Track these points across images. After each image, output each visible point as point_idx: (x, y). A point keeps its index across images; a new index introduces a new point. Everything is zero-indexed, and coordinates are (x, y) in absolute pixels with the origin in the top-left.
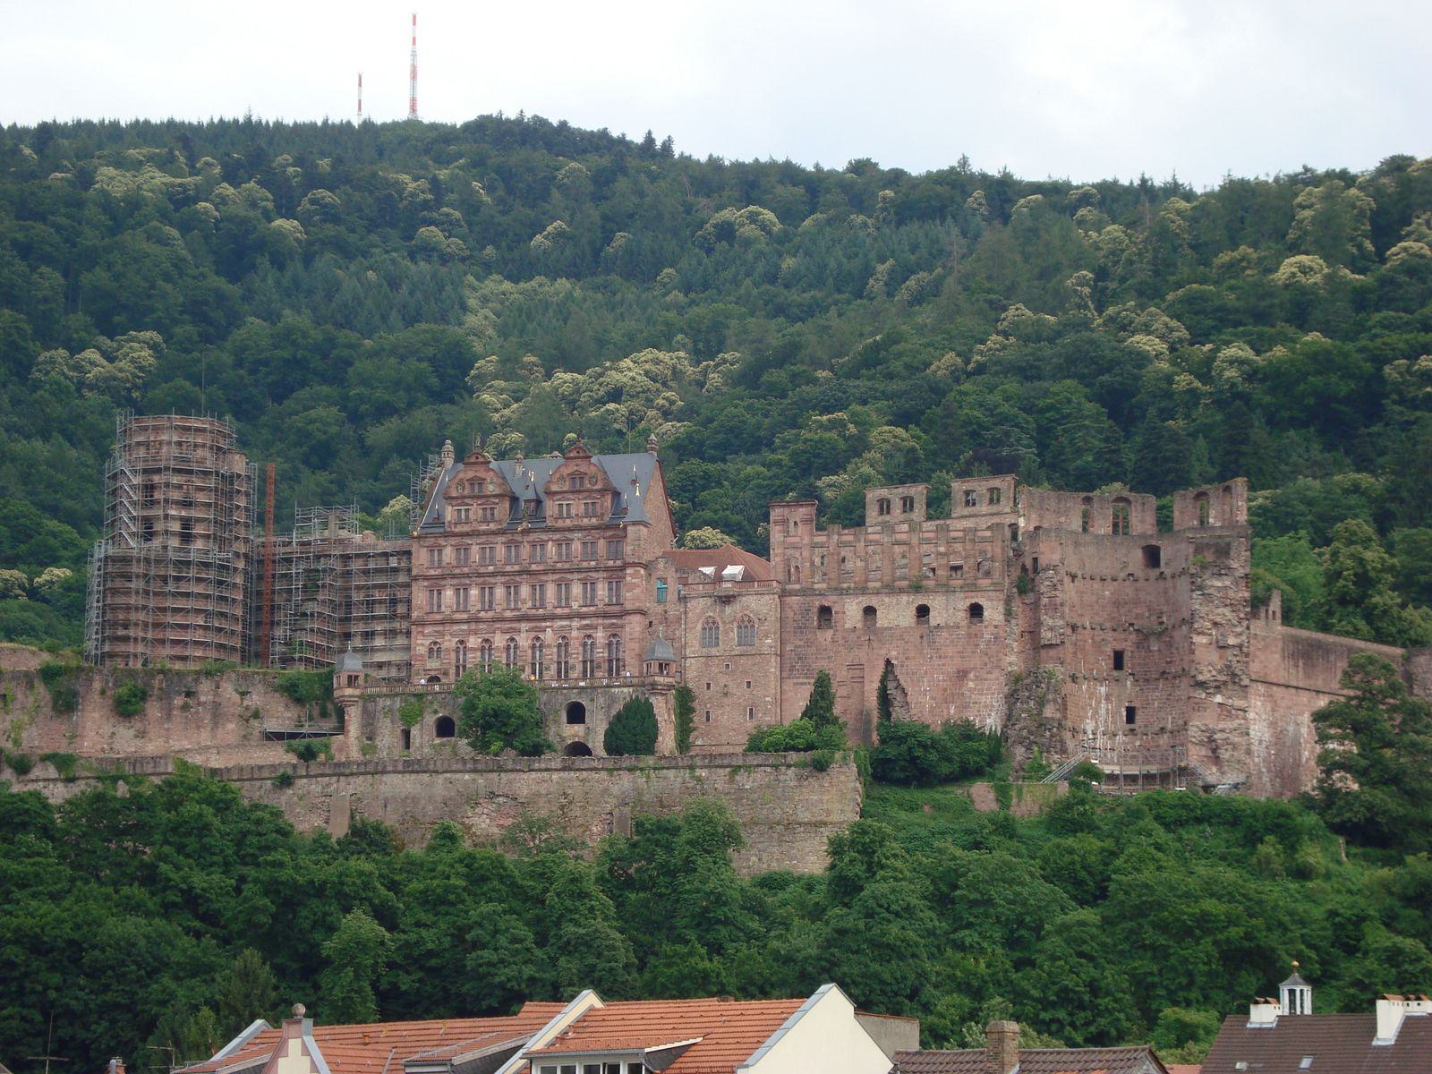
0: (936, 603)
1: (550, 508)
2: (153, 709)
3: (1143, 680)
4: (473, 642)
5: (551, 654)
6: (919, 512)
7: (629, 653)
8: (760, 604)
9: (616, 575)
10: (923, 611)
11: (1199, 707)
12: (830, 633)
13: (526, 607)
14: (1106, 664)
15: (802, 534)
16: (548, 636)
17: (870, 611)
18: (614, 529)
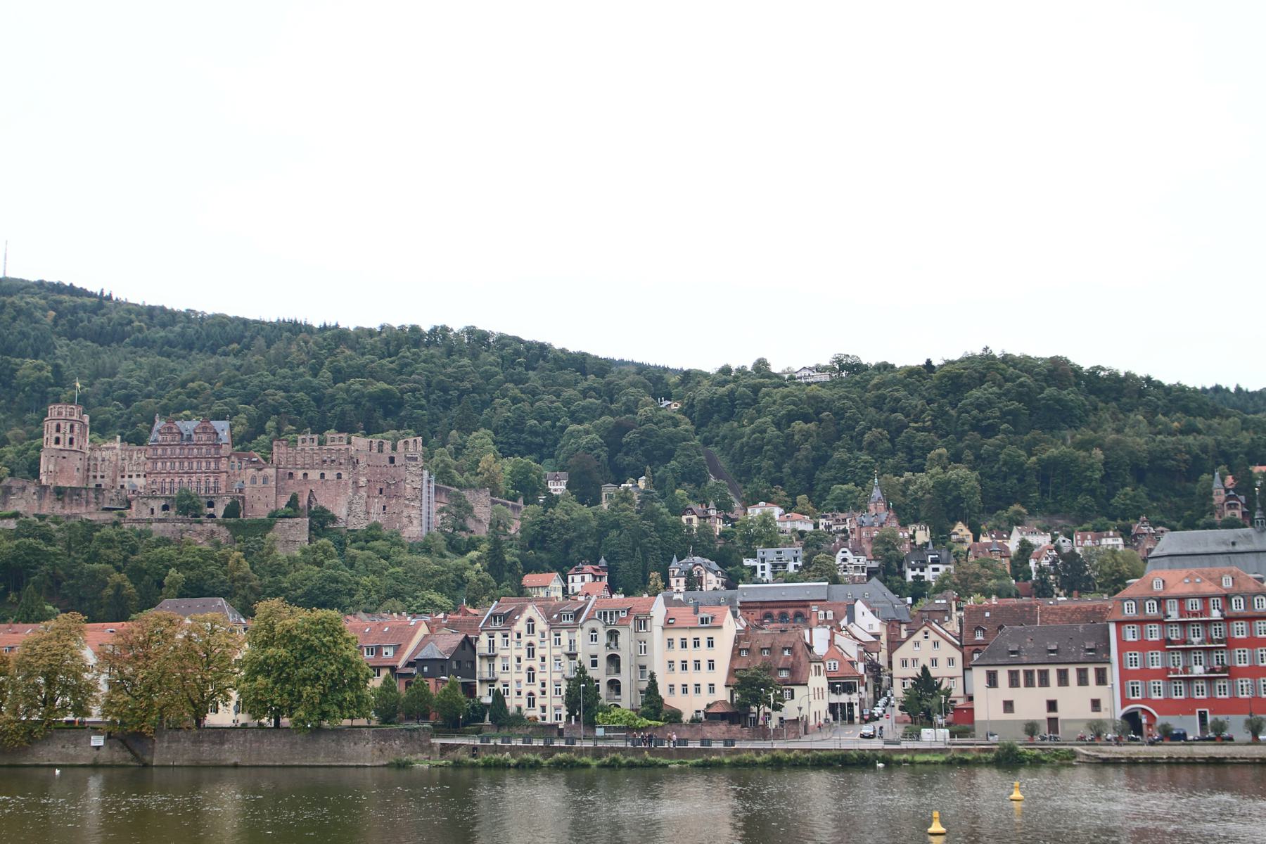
0: (327, 473)
1: (195, 437)
2: (67, 500)
3: (389, 497)
4: (168, 480)
5: (194, 485)
6: (316, 443)
7: (222, 485)
8: (271, 471)
9: (218, 460)
10: (322, 475)
11: (407, 506)
12: (291, 481)
13: (186, 469)
14: (377, 492)
15: (283, 450)
16: (194, 479)
17: (305, 475)
18: (218, 446)
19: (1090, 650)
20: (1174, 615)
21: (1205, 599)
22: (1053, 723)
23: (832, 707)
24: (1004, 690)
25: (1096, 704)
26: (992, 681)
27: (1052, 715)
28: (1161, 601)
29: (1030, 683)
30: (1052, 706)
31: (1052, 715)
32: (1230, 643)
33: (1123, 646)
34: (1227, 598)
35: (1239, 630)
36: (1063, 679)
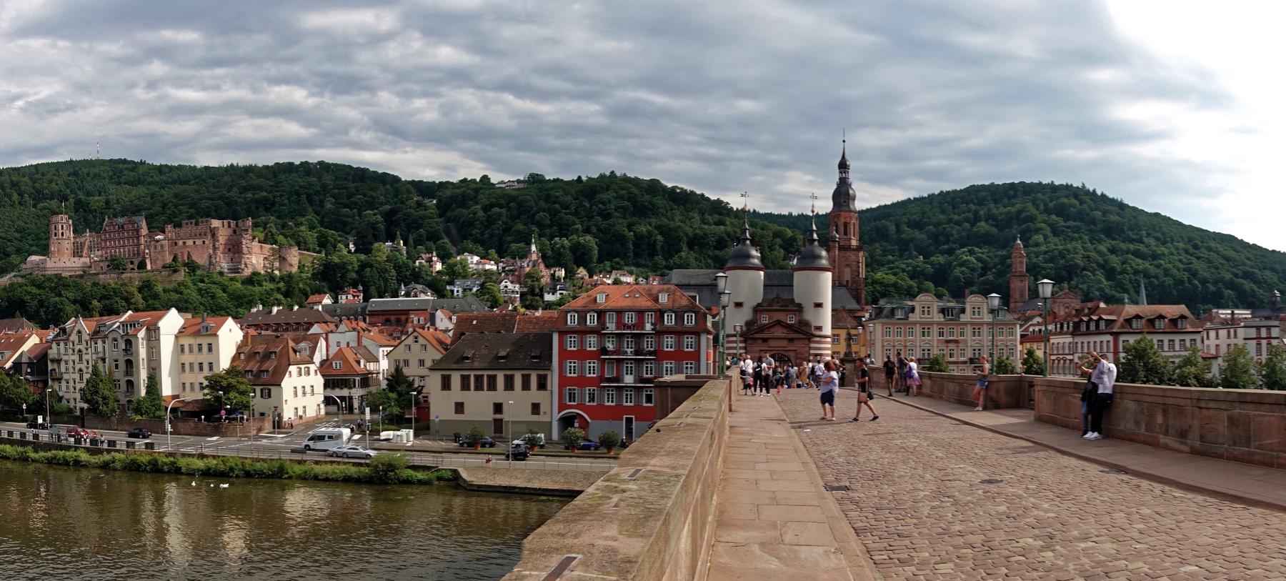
19: (535, 357)
20: (611, 327)
21: (641, 313)
22: (498, 424)
23: (328, 401)
24: (456, 393)
25: (536, 408)
26: (446, 384)
27: (498, 416)
28: (601, 314)
29: (479, 387)
30: (498, 408)
31: (498, 416)
32: (659, 355)
33: (564, 355)
34: (660, 313)
35: (669, 343)
36: (509, 385)
